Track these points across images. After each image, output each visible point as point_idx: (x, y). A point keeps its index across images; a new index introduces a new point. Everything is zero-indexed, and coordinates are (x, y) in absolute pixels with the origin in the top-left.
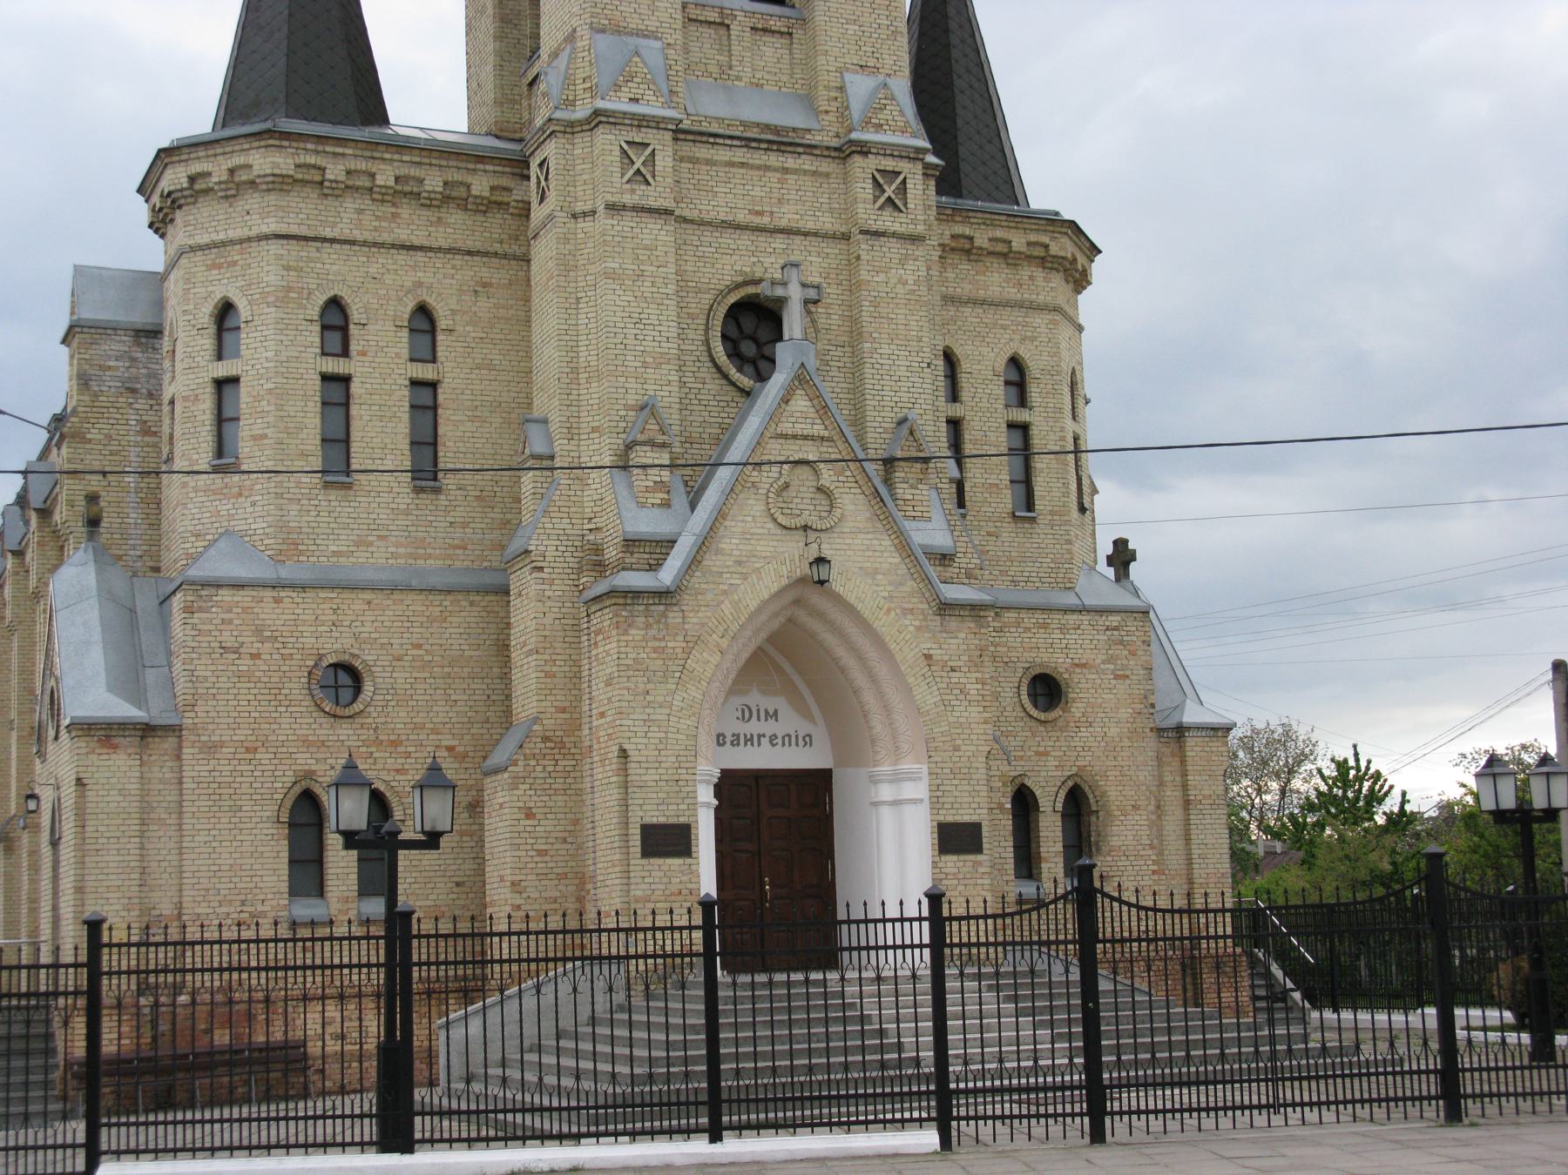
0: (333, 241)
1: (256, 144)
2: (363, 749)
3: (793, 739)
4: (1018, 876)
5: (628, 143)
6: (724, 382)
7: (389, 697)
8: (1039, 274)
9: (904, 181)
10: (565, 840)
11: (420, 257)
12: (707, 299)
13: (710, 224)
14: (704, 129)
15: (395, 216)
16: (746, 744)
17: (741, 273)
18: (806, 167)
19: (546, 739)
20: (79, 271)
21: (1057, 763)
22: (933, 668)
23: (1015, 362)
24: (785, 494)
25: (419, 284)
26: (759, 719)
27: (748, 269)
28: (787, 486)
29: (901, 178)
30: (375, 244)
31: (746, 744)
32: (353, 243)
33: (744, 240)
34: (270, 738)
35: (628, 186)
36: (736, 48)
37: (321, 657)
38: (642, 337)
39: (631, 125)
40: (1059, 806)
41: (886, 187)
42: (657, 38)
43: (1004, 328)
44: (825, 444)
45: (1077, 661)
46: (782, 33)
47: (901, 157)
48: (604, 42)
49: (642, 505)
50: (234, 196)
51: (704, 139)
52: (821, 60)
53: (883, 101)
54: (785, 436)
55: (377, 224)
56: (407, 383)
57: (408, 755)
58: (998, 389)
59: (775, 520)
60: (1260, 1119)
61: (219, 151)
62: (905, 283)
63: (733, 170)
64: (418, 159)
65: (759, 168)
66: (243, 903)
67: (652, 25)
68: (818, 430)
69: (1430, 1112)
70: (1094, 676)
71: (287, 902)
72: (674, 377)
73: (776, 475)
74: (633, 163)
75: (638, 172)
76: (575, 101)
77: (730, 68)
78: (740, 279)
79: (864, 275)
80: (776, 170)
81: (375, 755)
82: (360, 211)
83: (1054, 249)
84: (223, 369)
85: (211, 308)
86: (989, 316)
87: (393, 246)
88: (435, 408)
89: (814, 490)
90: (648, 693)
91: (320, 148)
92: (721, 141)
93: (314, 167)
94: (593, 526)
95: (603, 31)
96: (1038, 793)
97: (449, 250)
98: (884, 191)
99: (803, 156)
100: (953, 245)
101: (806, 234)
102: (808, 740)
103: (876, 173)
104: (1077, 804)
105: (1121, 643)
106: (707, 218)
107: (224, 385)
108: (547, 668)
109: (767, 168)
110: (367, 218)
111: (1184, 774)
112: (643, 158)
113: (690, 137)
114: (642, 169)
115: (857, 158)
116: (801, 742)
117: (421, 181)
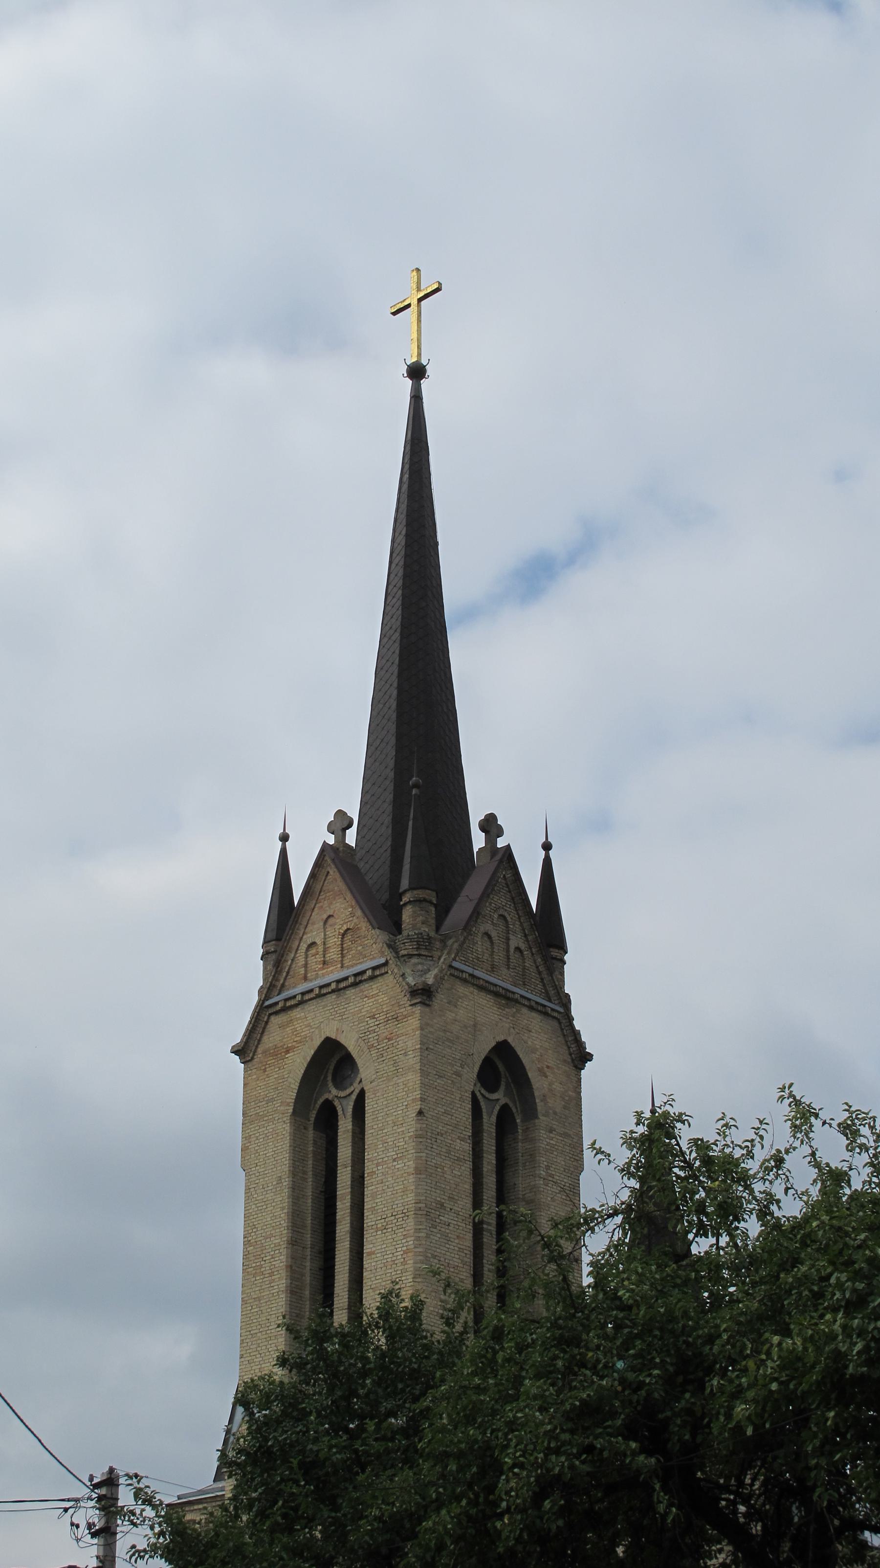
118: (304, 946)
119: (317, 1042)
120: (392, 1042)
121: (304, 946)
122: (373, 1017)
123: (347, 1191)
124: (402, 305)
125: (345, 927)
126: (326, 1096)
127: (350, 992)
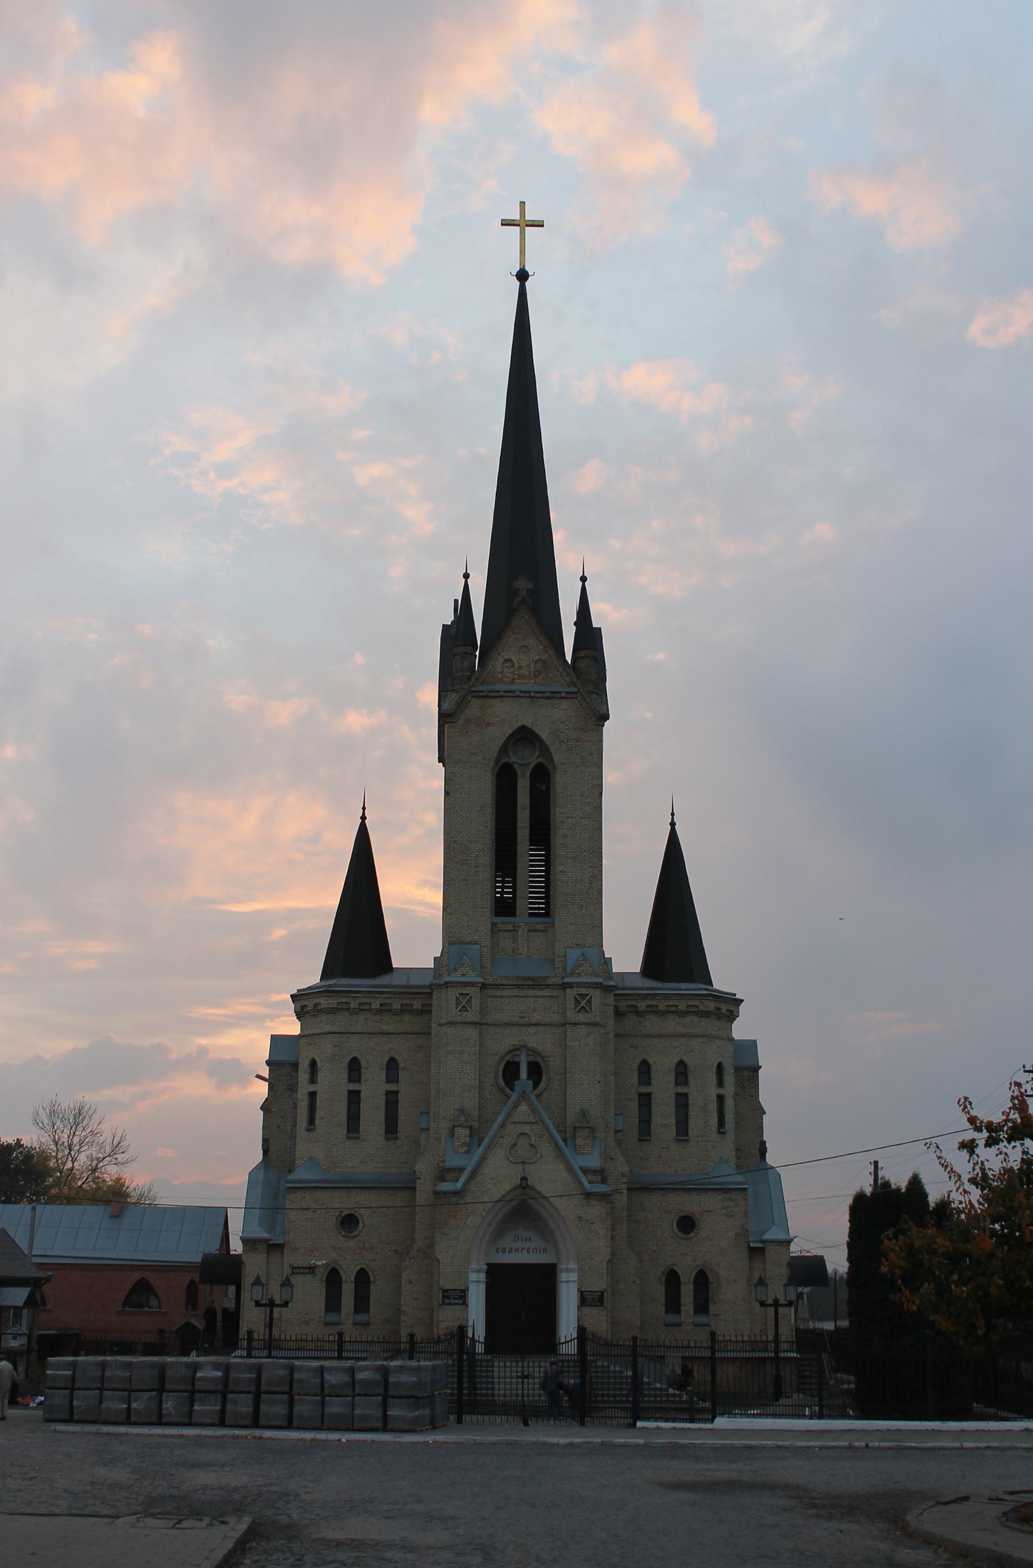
0: (354, 1033)
2: (358, 1251)
4: (667, 1312)
5: (459, 994)
6: (502, 1094)
7: (370, 1229)
8: (695, 1019)
10: (425, 1294)
13: (499, 1025)
14: (498, 983)
16: (515, 1252)
17: (515, 1045)
18: (547, 994)
19: (419, 1251)
21: (692, 1259)
23: (681, 1063)
24: (515, 1147)
26: (522, 1241)
28: (515, 1144)
29: (589, 996)
30: (372, 1033)
31: (515, 1252)
32: (363, 1033)
34: (320, 1246)
35: (459, 1013)
39: (461, 986)
40: (692, 1280)
41: (581, 1002)
42: (479, 944)
43: (676, 1047)
44: (534, 1125)
45: (705, 1209)
46: (543, 931)
47: (588, 987)
49: (456, 1153)
50: (317, 1015)
51: (498, 987)
53: (582, 962)
54: (515, 1123)
55: (373, 1024)
56: (384, 1092)
57: (377, 1253)
58: (671, 1077)
59: (509, 1160)
61: (311, 997)
63: (513, 999)
64: (389, 996)
65: (524, 997)
66: (306, 1314)
67: (476, 938)
68: (532, 1118)
71: (324, 1314)
73: (511, 1140)
74: (462, 1003)
75: (464, 1006)
76: (442, 974)
77: (518, 950)
78: (513, 1048)
79: (569, 1043)
80: (533, 997)
81: (364, 1253)
82: (366, 1019)
83: (702, 1008)
84: (312, 1088)
85: (308, 1062)
87: (380, 1033)
88: (397, 1102)
91: (348, 995)
92: (505, 987)
94: (442, 1160)
95: (453, 944)
96: (680, 1273)
97: (404, 1033)
98: (581, 1003)
99: (545, 990)
100: (648, 1010)
101: (545, 1025)
102: (545, 1250)
103: (577, 997)
104: (702, 1280)
107: (313, 1095)
109: (527, 997)
112: (466, 1001)
114: (466, 1005)
115: (567, 990)
116: (542, 1251)
117: (391, 1005)
118: (501, 660)
119: (515, 727)
120: (580, 743)
121: (501, 660)
124: (512, 223)
125: (538, 657)
127: (542, 701)
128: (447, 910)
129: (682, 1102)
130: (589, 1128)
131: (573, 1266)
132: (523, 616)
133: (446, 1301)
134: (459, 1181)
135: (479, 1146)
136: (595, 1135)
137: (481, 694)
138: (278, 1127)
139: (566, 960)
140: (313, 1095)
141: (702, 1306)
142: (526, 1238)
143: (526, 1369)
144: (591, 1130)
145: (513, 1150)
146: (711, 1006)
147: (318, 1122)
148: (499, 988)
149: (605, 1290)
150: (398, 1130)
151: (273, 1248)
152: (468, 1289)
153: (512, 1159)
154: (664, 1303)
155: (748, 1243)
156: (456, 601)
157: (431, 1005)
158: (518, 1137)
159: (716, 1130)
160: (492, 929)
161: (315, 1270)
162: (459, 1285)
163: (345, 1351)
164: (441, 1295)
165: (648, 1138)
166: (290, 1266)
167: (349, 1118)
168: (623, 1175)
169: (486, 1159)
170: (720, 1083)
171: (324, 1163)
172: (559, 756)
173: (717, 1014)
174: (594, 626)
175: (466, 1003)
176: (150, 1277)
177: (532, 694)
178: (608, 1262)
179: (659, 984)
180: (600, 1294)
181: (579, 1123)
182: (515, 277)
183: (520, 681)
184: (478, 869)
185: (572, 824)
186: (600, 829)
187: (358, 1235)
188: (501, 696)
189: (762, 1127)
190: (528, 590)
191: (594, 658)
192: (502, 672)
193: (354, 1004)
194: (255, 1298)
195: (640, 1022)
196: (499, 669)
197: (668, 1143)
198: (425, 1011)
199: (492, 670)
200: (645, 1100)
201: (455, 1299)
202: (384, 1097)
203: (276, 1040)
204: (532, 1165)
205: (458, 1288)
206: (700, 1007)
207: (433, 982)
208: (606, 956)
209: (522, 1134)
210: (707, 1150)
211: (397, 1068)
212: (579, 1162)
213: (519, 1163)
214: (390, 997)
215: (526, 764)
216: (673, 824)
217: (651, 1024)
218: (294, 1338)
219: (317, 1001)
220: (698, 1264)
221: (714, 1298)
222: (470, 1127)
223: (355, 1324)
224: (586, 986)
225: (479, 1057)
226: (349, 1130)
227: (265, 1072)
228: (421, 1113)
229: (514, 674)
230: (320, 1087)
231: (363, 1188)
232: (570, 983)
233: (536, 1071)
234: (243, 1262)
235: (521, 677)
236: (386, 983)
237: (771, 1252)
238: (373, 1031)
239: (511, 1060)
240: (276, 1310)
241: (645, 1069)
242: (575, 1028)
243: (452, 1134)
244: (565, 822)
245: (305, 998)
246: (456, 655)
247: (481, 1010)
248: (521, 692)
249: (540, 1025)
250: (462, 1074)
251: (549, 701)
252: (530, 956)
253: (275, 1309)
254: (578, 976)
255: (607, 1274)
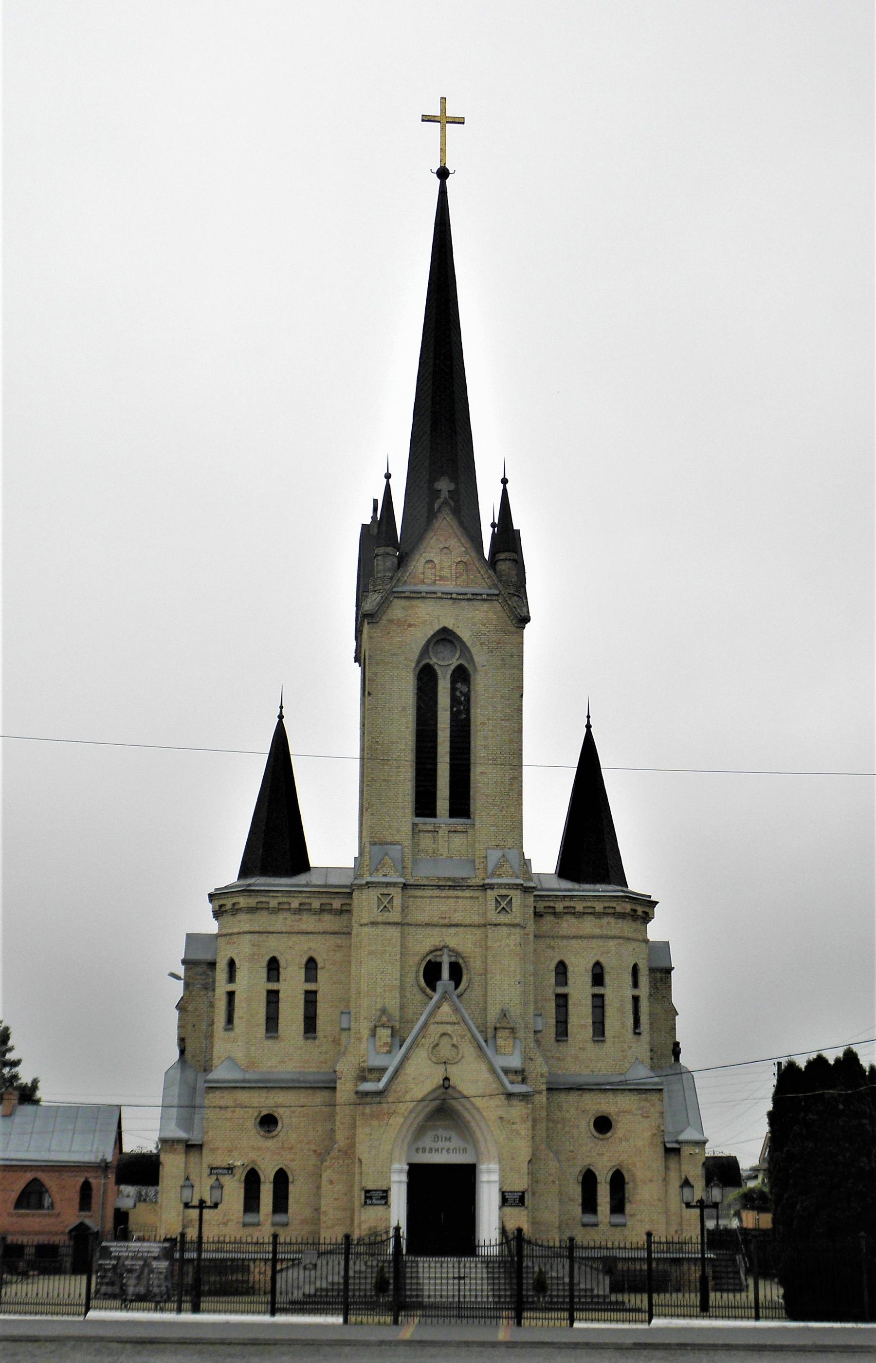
0: (273, 933)
1: (241, 894)
3: (458, 1150)
5: (381, 894)
8: (612, 920)
9: (512, 898)
11: (311, 936)
12: (417, 958)
13: (420, 925)
14: (419, 883)
15: (301, 919)
16: (435, 1152)
18: (468, 895)
20: (189, 936)
22: (503, 1123)
23: (598, 964)
24: (437, 1048)
25: (310, 948)
26: (442, 1140)
27: (437, 944)
28: (437, 1045)
29: (509, 898)
31: (435, 1152)
32: (282, 933)
33: (436, 930)
35: (380, 914)
36: (441, 841)
37: (260, 1112)
38: (383, 979)
40: (608, 1179)
41: (502, 903)
44: (457, 1025)
46: (464, 832)
48: (377, 848)
49: (378, 1053)
50: (235, 914)
51: (419, 887)
52: (477, 845)
54: (438, 1023)
56: (303, 992)
58: (588, 979)
60: (453, 1320)
61: (229, 896)
62: (510, 946)
64: (308, 895)
65: (445, 897)
67: (397, 838)
68: (454, 1019)
69: (511, 1322)
70: (630, 1117)
71: (242, 1216)
72: (398, 995)
75: (385, 907)
76: (363, 875)
78: (433, 948)
79: (489, 944)
81: (282, 1154)
82: (285, 919)
84: (230, 987)
86: (585, 943)
87: (299, 933)
88: (316, 1002)
89: (450, 1046)
90: (371, 1134)
91: (267, 895)
92: (427, 888)
93: (265, 902)
95: (375, 844)
96: (597, 1173)
97: (324, 933)
99: (466, 891)
100: (566, 911)
101: (466, 926)
102: (465, 1150)
104: (618, 1181)
105: (646, 1100)
106: (419, 923)
108: (342, 1121)
109: (448, 897)
110: (288, 922)
111: (680, 1164)
113: (413, 887)
115: (489, 892)
116: (461, 1151)
117: (310, 904)
119: (437, 627)
122: (484, 625)
123: (447, 726)
126: (428, 661)
127: (464, 603)
128: (369, 810)
129: (599, 1003)
130: (510, 1028)
131: (494, 1166)
132: (445, 518)
133: (369, 1202)
134: (382, 1081)
135: (401, 1046)
136: (515, 1036)
137: (402, 595)
138: (194, 1026)
139: (487, 861)
140: (231, 995)
141: (618, 1206)
142: (445, 1138)
143: (462, 1270)
144: (511, 1030)
145: (435, 1050)
146: (628, 907)
147: (236, 1021)
148: (420, 889)
149: (526, 1191)
150: (317, 1030)
151: (192, 1148)
152: (389, 1189)
153: (433, 1059)
154: (580, 1203)
155: (664, 1143)
156: (376, 501)
157: (350, 905)
158: (439, 1040)
159: (632, 1031)
160: (413, 829)
161: (234, 1171)
162: (380, 1185)
163: (279, 1253)
164: (363, 1198)
165: (565, 1038)
166: (209, 1167)
167: (268, 1019)
168: (542, 1076)
169: (408, 1059)
170: (636, 985)
171: (242, 1062)
172: (480, 656)
173: (633, 916)
174: (515, 528)
175: (388, 903)
176: (41, 1176)
177: (454, 596)
178: (528, 1163)
179: (576, 886)
180: (521, 1194)
181: (500, 1023)
182: (435, 175)
183: (442, 582)
184: (399, 770)
185: (493, 726)
186: (520, 731)
187: (276, 1135)
188: (423, 597)
189: (675, 1029)
190: (449, 491)
191: (515, 561)
192: (423, 573)
193: (273, 903)
194: (184, 1200)
195: (558, 923)
196: (421, 570)
197: (585, 1044)
198: (345, 911)
199: (414, 571)
200: (562, 1001)
201: (378, 1199)
202: (303, 996)
203: (192, 939)
204: (454, 1066)
205: (379, 1188)
206: (617, 909)
207: (354, 883)
208: (526, 858)
209: (444, 1034)
210: (623, 1051)
211: (316, 968)
212: (500, 1062)
213: (441, 1063)
214: (309, 897)
215: (448, 665)
216: (588, 727)
217: (568, 925)
218: (211, 1240)
219: (235, 900)
220: (615, 1164)
221: (630, 1198)
222: (392, 1027)
223: (274, 1224)
224: (507, 887)
225: (401, 958)
226: (267, 1030)
227: (181, 970)
228: (342, 1013)
229: (435, 576)
230: (240, 986)
231: (281, 1088)
232: (492, 884)
233: (456, 972)
234: (161, 1163)
235: (442, 578)
236: (304, 882)
237: (686, 1150)
238: (293, 931)
239: (433, 960)
240: (205, 1211)
241: (562, 969)
242: (496, 929)
243: (373, 1033)
244: (486, 723)
245: (223, 897)
246: (377, 555)
247: (403, 910)
248: (443, 593)
249: (461, 925)
250: (384, 974)
251: (471, 603)
252: (450, 857)
253: (204, 1211)
254: (499, 878)
255: (528, 1173)
